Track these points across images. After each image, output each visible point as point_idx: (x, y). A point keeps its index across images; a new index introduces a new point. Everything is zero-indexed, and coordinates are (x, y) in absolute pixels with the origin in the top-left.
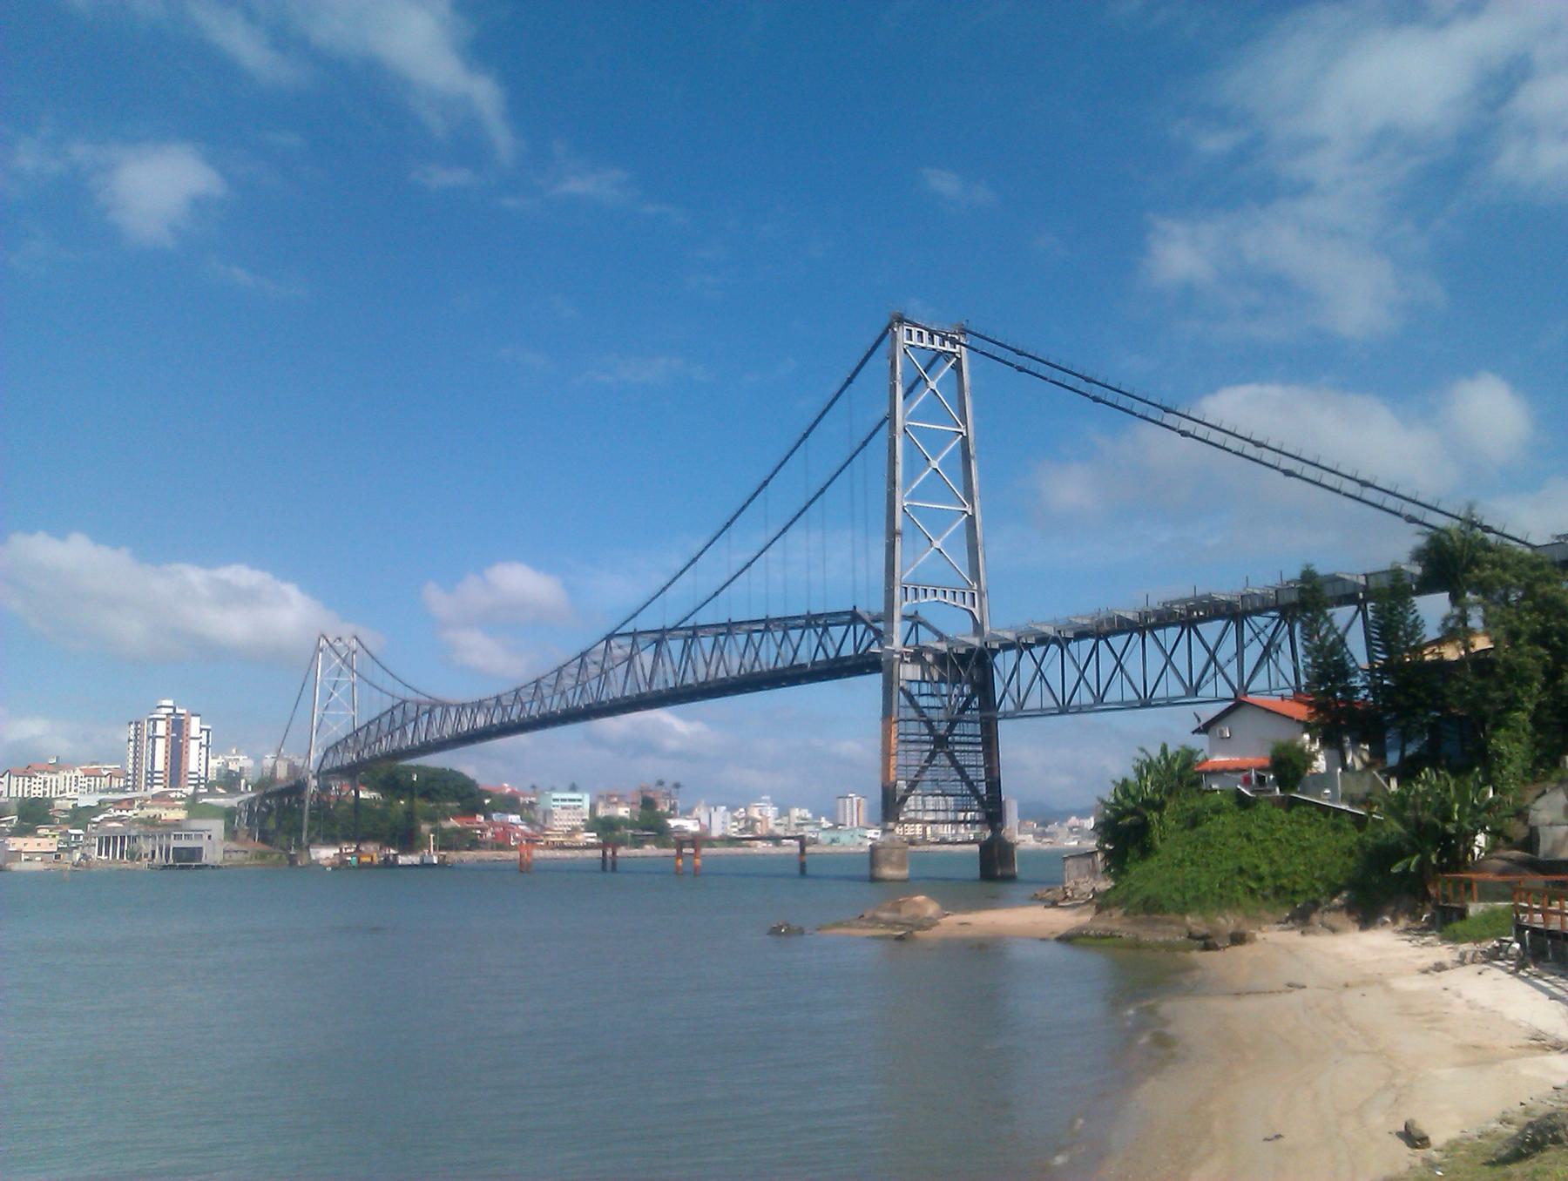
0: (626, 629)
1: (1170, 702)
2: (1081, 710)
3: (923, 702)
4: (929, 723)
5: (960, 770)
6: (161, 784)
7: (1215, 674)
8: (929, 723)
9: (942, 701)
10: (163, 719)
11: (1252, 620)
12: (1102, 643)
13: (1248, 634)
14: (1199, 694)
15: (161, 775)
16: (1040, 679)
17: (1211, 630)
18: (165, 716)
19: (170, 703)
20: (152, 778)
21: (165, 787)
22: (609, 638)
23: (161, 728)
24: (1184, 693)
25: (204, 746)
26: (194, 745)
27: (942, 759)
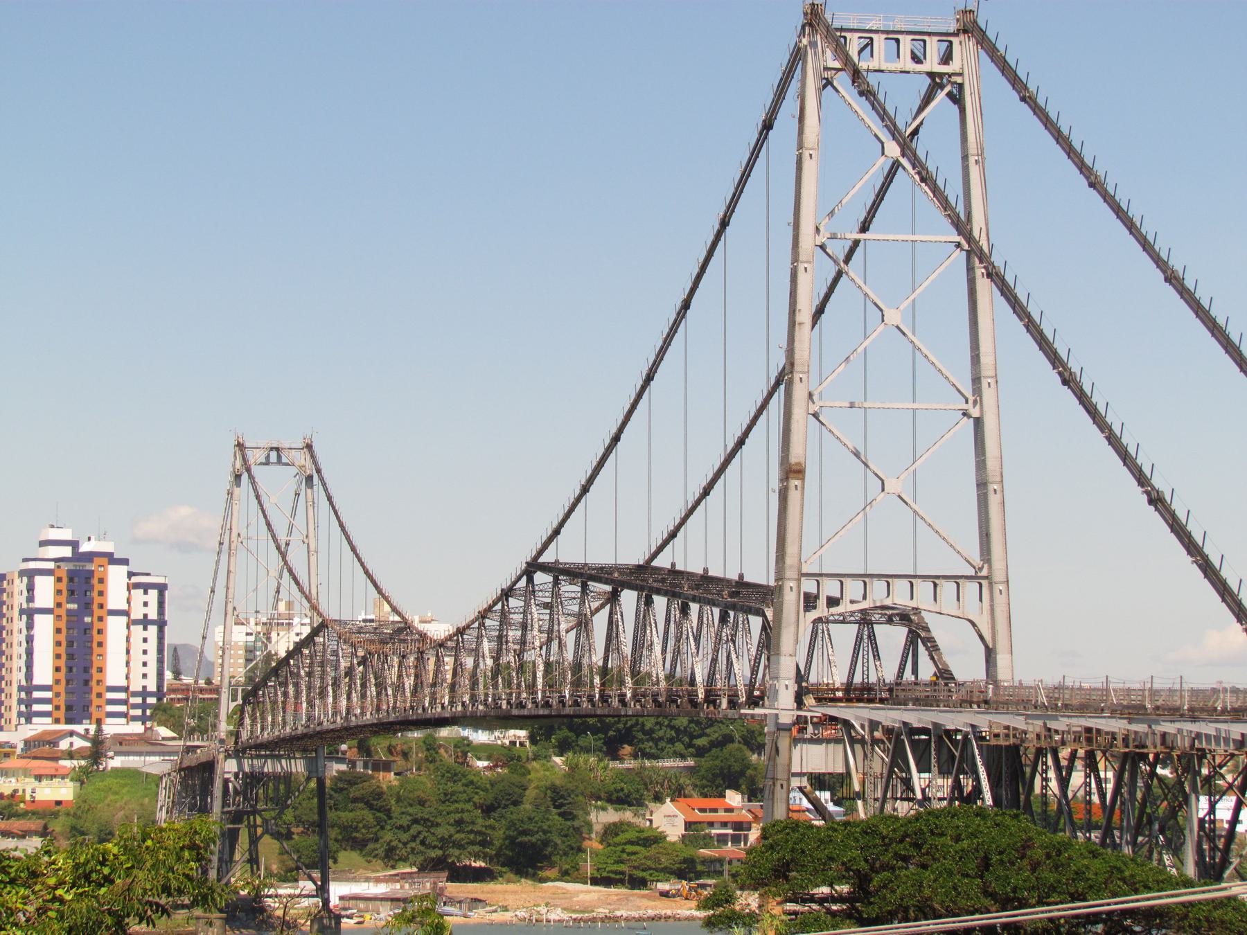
15: (49, 695)
18: (51, 565)
20: (29, 703)
21: (57, 721)
23: (45, 593)
25: (153, 622)
26: (115, 628)
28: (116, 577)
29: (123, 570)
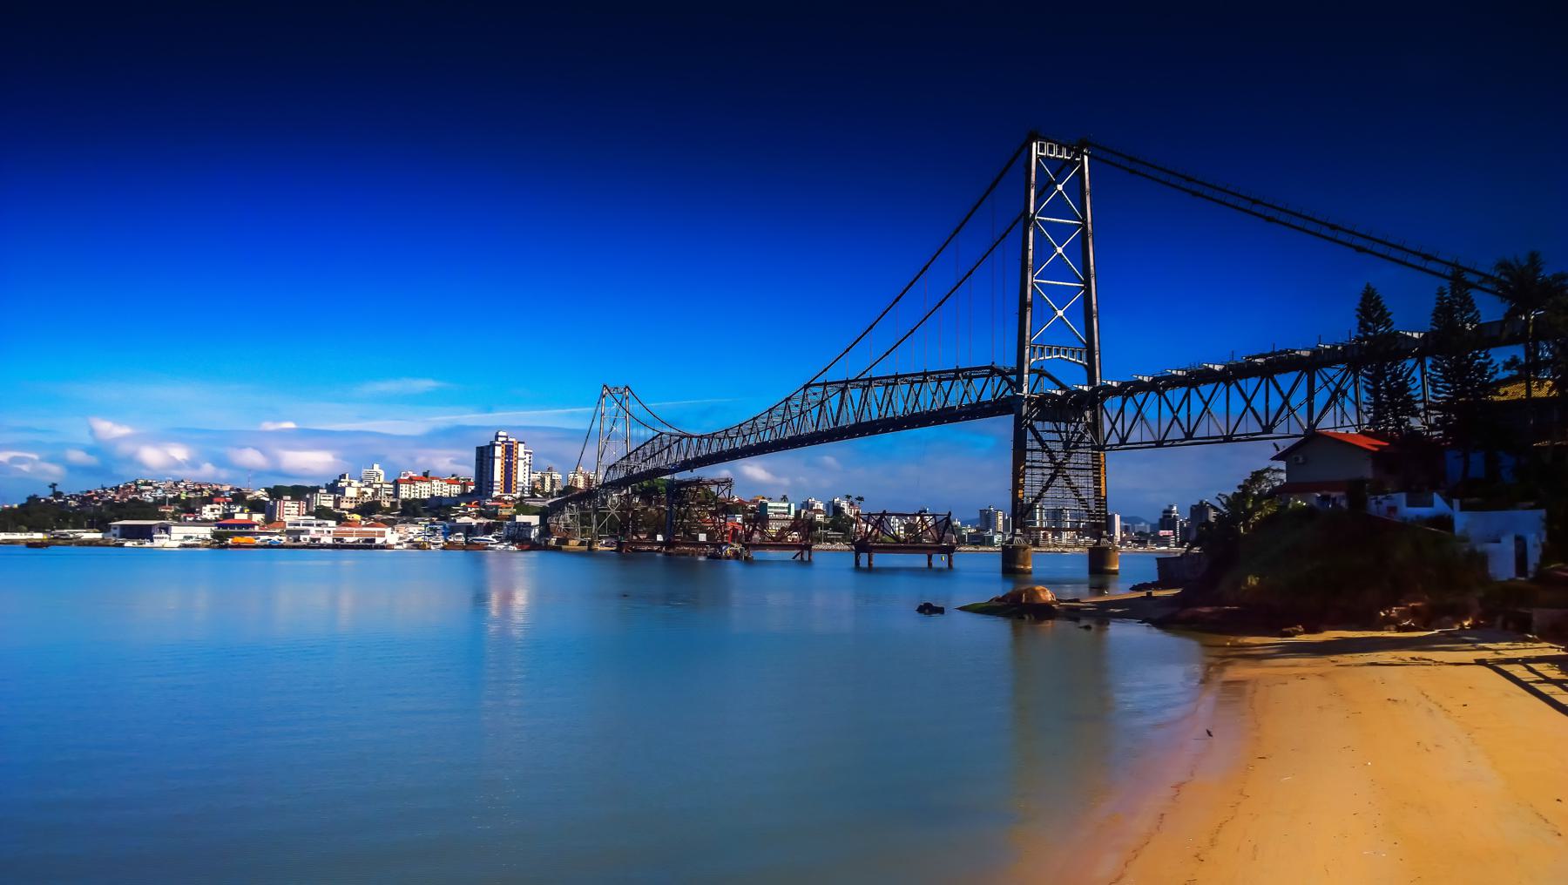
0: (821, 380)
1: (1250, 437)
2: (1173, 443)
3: (1045, 436)
4: (1050, 453)
5: (1075, 490)
6: (497, 490)
7: (1288, 416)
8: (1050, 453)
9: (1061, 436)
10: (500, 445)
11: (1323, 372)
12: (1193, 391)
13: (1318, 382)
14: (1274, 431)
16: (1142, 419)
17: (1285, 380)
18: (500, 443)
19: (504, 434)
22: (806, 387)
24: (1261, 430)
26: (521, 463)
27: (1060, 481)
28: (521, 446)
29: (523, 445)
